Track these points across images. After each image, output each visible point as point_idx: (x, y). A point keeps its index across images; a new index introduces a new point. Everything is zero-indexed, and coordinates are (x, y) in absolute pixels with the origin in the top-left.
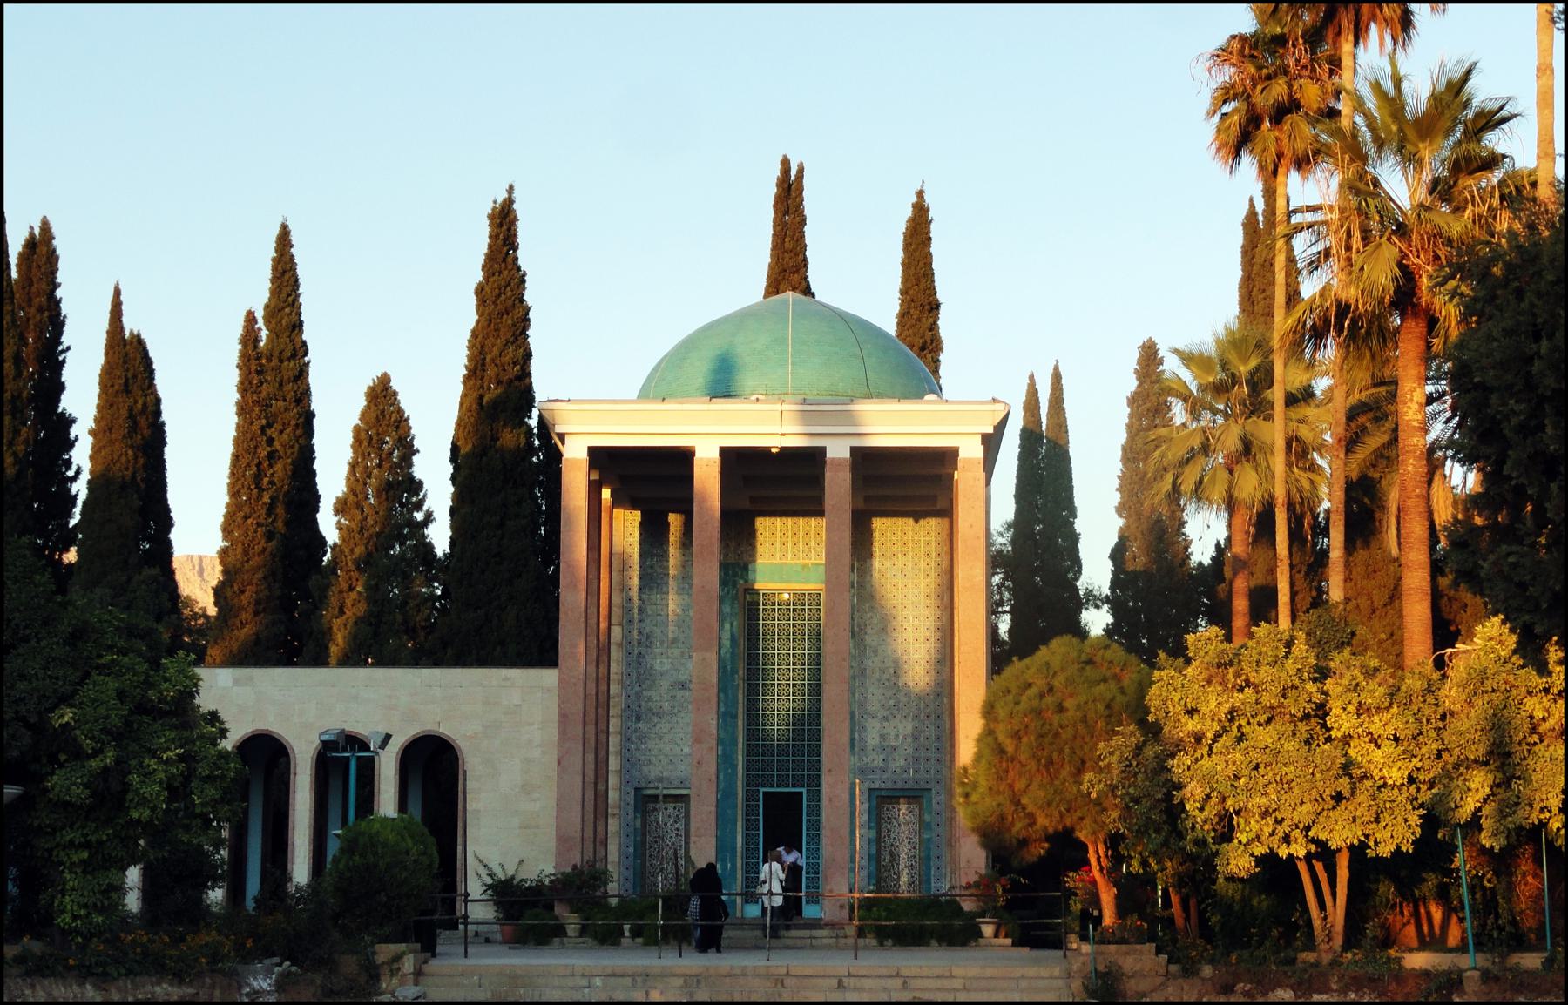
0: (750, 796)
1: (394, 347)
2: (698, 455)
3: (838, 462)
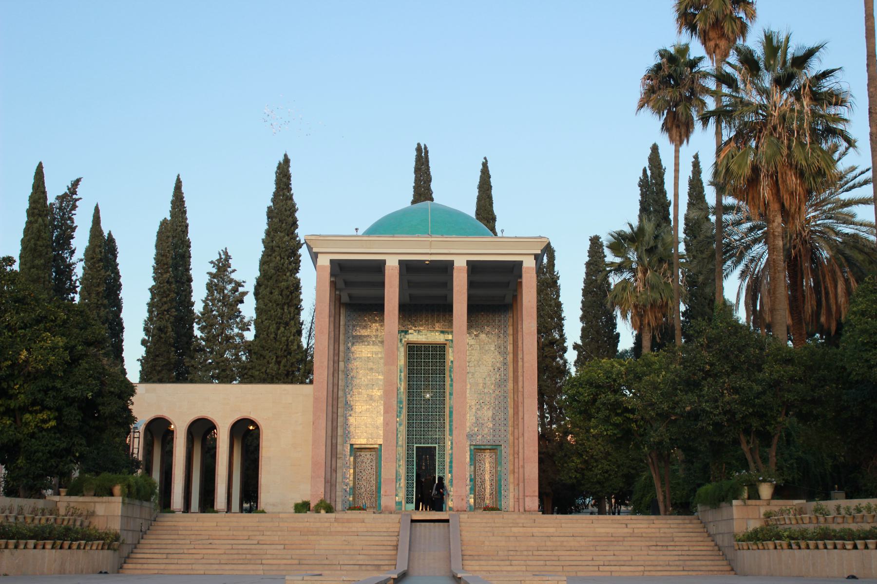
0: (409, 448)
1: (229, 239)
2: (387, 264)
3: (460, 268)
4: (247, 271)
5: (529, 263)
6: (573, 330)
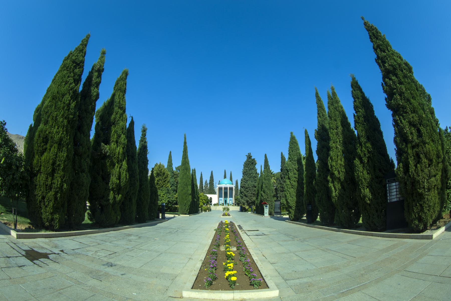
4: (208, 182)
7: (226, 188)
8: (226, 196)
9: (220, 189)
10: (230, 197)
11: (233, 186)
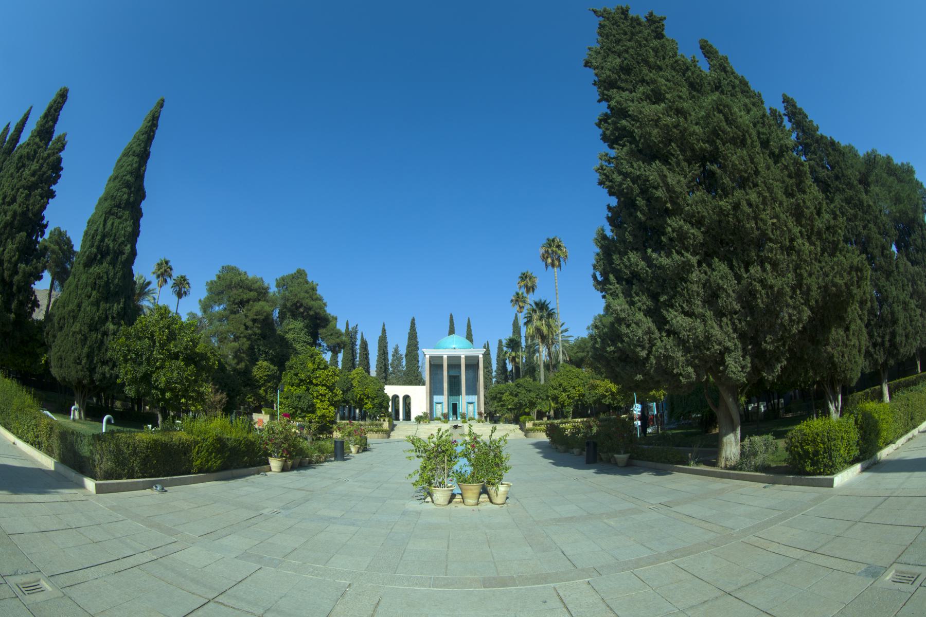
1: (398, 342)
4: (403, 351)
5: (481, 356)
6: (494, 366)
7: (454, 363)
8: (454, 390)
9: (436, 365)
10: (468, 393)
11: (479, 353)
